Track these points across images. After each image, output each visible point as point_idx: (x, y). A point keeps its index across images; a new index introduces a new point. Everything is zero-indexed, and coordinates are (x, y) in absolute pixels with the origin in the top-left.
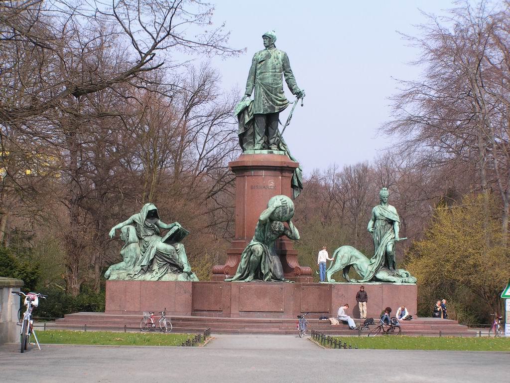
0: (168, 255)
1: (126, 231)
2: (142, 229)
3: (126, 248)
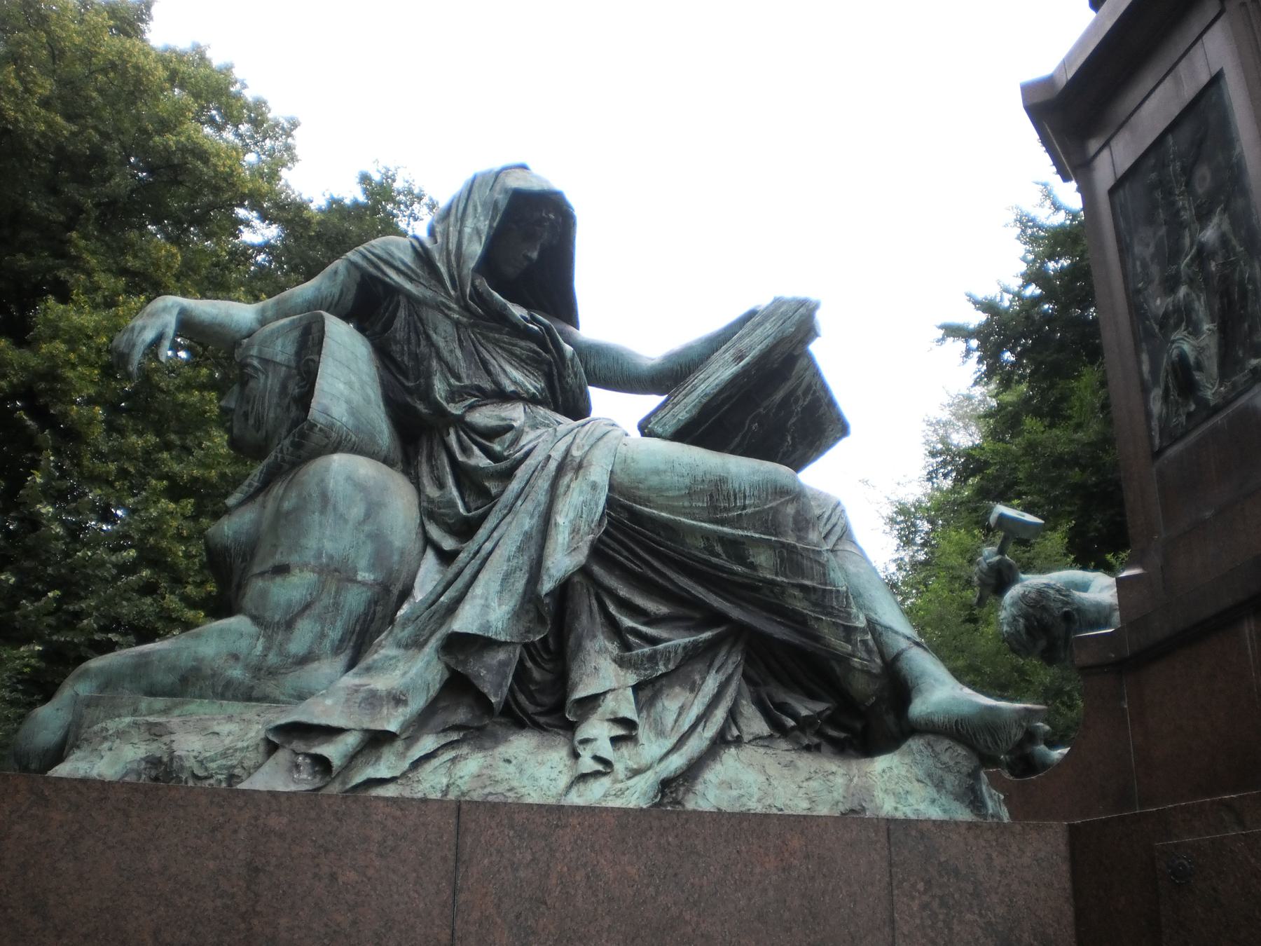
0: (736, 548)
1: (283, 350)
2: (443, 335)
3: (278, 489)
